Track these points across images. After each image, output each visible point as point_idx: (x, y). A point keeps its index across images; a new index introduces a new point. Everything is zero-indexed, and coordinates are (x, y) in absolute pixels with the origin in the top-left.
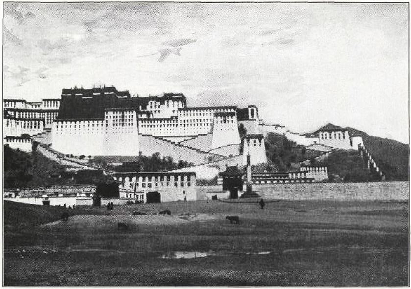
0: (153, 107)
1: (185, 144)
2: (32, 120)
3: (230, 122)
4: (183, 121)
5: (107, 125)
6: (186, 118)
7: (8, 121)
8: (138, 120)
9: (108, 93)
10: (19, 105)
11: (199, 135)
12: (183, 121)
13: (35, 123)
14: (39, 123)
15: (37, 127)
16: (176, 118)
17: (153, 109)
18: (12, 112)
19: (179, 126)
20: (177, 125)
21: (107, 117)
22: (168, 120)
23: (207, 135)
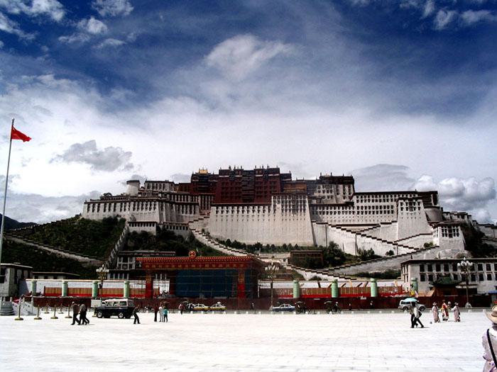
2: (187, 204)
5: (275, 210)
6: (364, 204)
10: (167, 189)
11: (382, 223)
16: (352, 204)
17: (322, 194)
23: (390, 223)
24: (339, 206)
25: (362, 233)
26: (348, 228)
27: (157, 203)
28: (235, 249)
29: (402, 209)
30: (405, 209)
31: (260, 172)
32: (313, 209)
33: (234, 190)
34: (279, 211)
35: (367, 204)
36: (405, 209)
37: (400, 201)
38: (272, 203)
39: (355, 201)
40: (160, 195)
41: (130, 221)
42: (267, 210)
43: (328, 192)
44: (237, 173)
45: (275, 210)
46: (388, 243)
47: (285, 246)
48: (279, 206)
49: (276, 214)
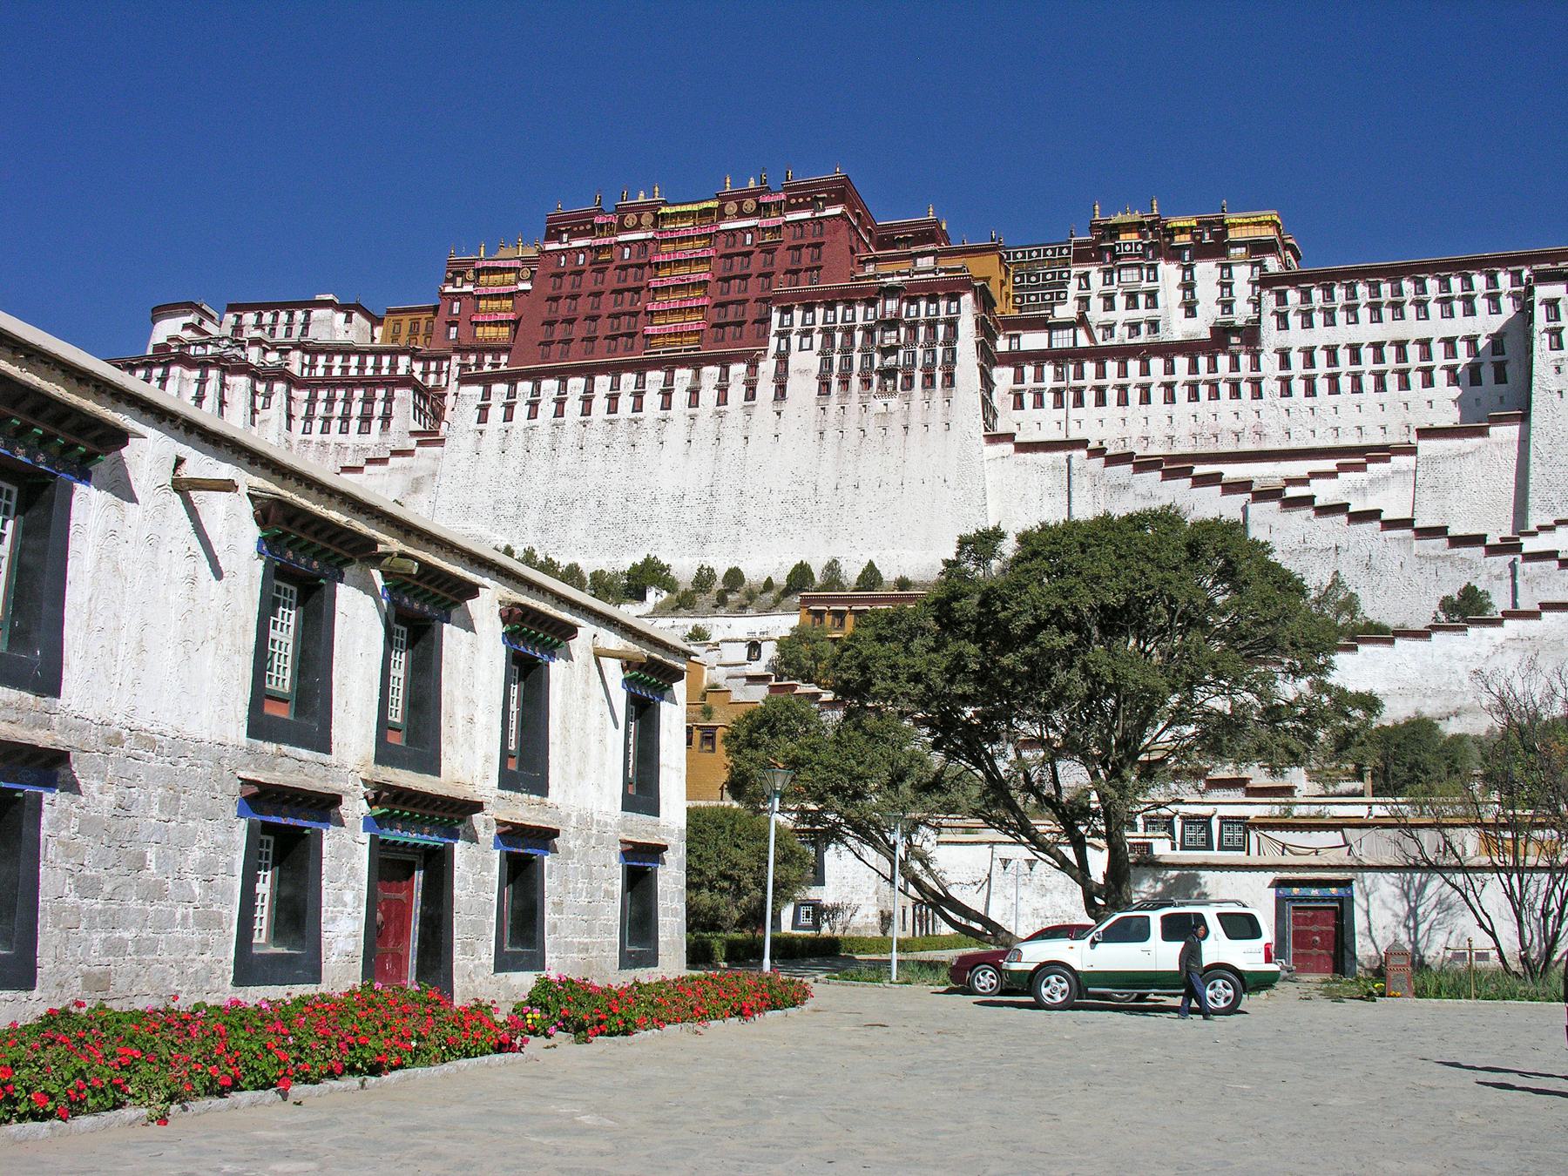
0: (1096, 304)
1: (1324, 492)
4: (1296, 359)
6: (1320, 335)
7: (202, 382)
8: (989, 359)
9: (807, 215)
12: (1296, 359)
13: (368, 401)
14: (389, 400)
15: (376, 424)
16: (1251, 334)
18: (273, 357)
19: (1271, 386)
20: (1256, 383)
21: (784, 335)
22: (1190, 348)
24: (1168, 351)
25: (1292, 492)
27: (175, 370)
31: (750, 205)
32: (1019, 378)
33: (608, 304)
34: (803, 386)
35: (1343, 333)
38: (773, 341)
39: (1269, 323)
42: (737, 391)
43: (1132, 300)
44: (630, 219)
46: (1457, 541)
47: (801, 574)
48: (805, 362)
49: (786, 407)
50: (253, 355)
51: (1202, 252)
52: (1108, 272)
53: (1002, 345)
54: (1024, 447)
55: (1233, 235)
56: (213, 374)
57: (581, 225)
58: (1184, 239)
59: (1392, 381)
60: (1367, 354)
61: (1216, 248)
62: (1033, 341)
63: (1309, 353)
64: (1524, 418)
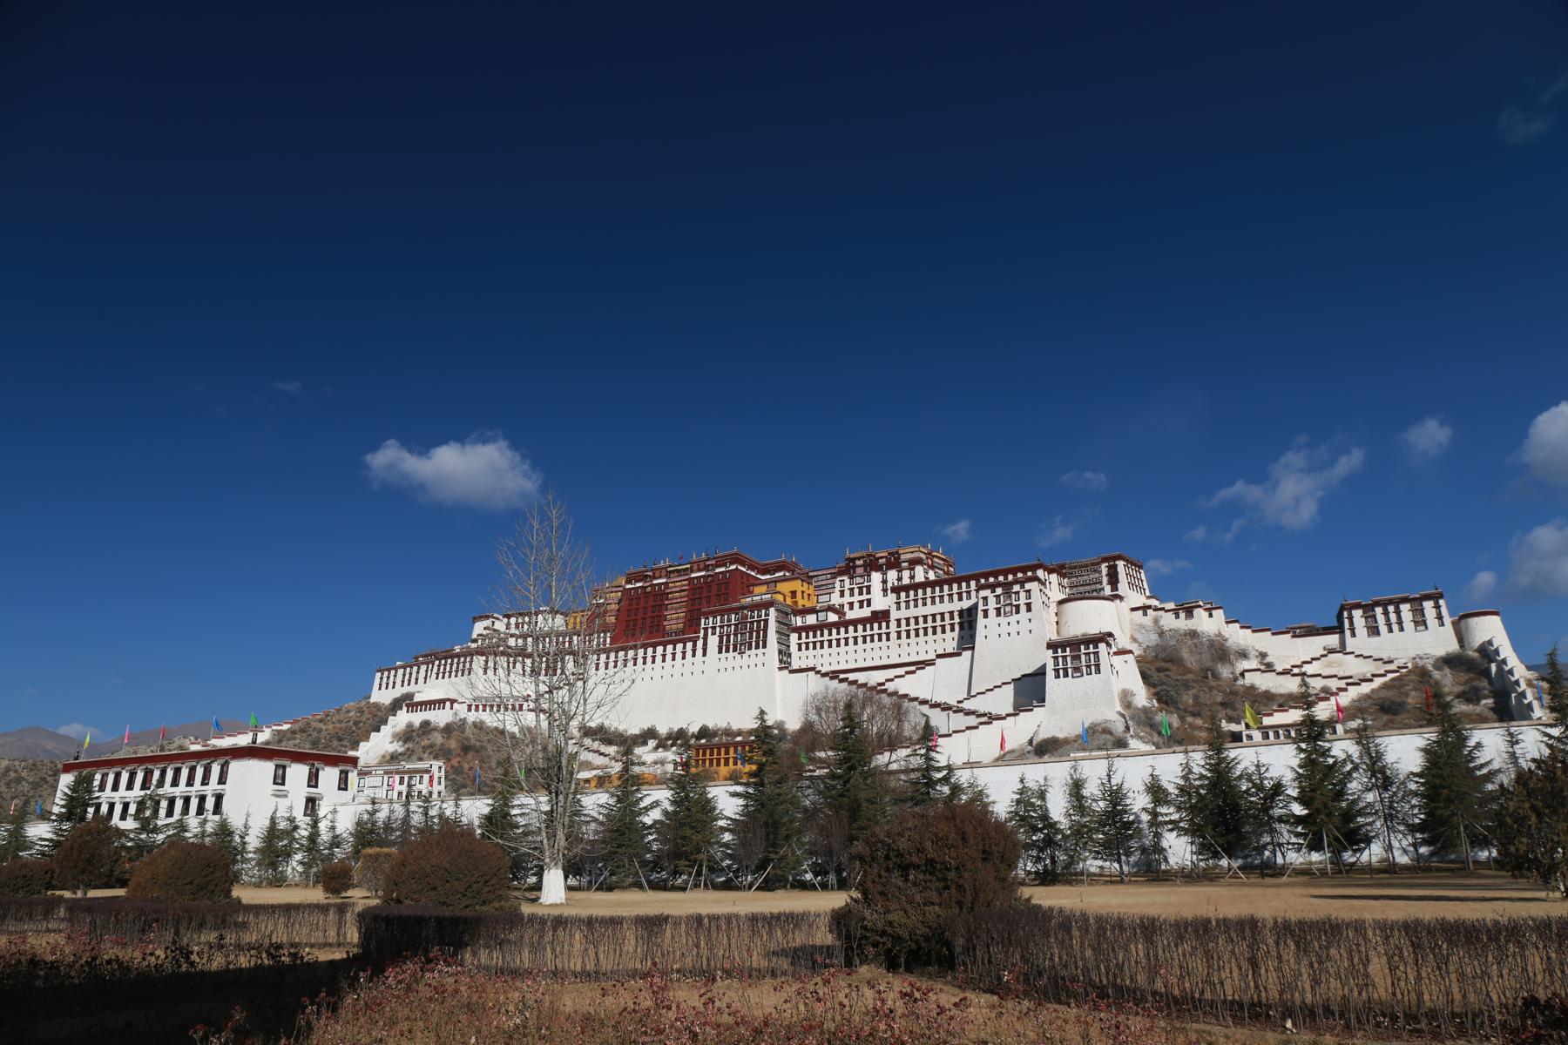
0: (847, 593)
1: (890, 686)
3: (1023, 608)
4: (903, 623)
5: (704, 654)
6: (912, 612)
11: (939, 656)
12: (903, 623)
17: (847, 599)
19: (893, 636)
20: (888, 634)
21: (706, 629)
26: (852, 677)
28: (603, 749)
29: (986, 616)
30: (992, 613)
35: (920, 611)
36: (992, 613)
37: (983, 593)
40: (512, 642)
41: (416, 699)
43: (861, 593)
45: (704, 654)
48: (713, 641)
50: (512, 642)
51: (890, 566)
52: (851, 578)
53: (799, 621)
54: (792, 672)
55: (903, 557)
56: (491, 658)
57: (642, 577)
58: (882, 561)
59: (939, 630)
60: (930, 619)
61: (894, 563)
62: (811, 619)
63: (908, 620)
64: (973, 648)
